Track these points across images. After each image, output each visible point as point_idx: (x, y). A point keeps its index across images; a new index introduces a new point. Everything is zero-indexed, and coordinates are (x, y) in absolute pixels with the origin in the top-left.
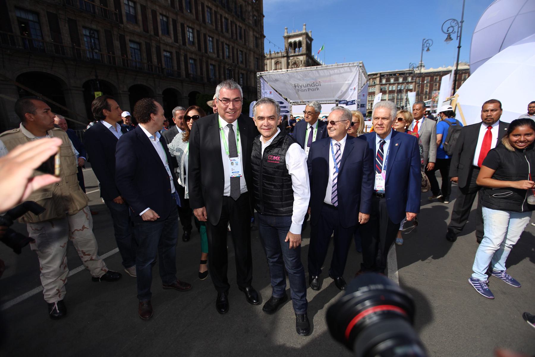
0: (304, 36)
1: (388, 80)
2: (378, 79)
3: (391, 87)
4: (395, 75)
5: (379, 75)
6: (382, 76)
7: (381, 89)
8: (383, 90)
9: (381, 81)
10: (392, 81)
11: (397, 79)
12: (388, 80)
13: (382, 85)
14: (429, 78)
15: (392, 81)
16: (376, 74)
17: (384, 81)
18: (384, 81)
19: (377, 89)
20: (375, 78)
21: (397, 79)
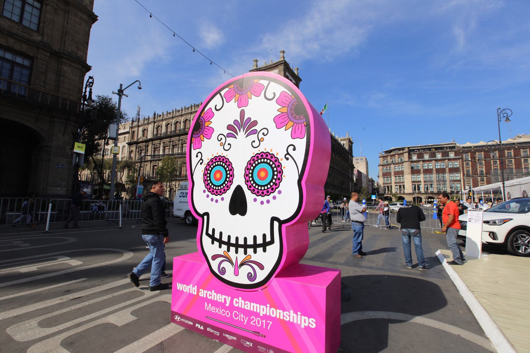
0: (282, 67)
1: (420, 156)
2: (406, 155)
3: (425, 165)
4: (429, 149)
5: (406, 150)
6: (411, 151)
7: (412, 168)
8: (415, 168)
9: (410, 157)
10: (426, 157)
11: (433, 155)
12: (420, 156)
13: (412, 162)
14: (483, 153)
15: (426, 157)
16: (403, 149)
17: (415, 158)
18: (415, 158)
19: (406, 168)
20: (402, 154)
21: (433, 155)
